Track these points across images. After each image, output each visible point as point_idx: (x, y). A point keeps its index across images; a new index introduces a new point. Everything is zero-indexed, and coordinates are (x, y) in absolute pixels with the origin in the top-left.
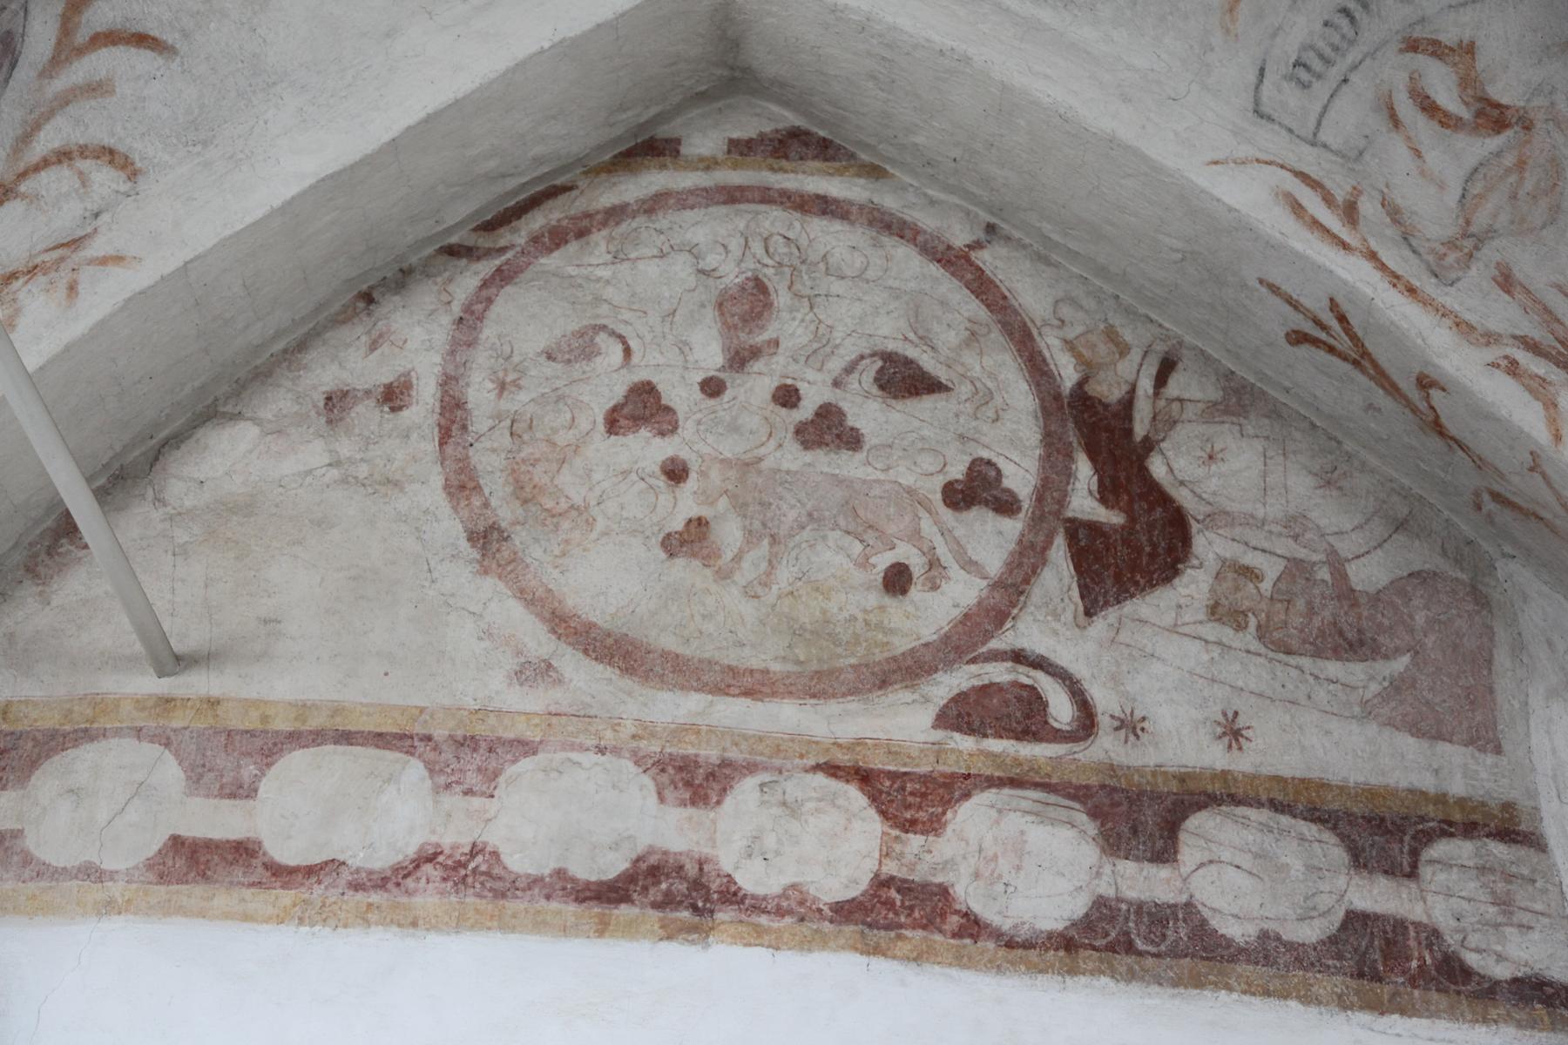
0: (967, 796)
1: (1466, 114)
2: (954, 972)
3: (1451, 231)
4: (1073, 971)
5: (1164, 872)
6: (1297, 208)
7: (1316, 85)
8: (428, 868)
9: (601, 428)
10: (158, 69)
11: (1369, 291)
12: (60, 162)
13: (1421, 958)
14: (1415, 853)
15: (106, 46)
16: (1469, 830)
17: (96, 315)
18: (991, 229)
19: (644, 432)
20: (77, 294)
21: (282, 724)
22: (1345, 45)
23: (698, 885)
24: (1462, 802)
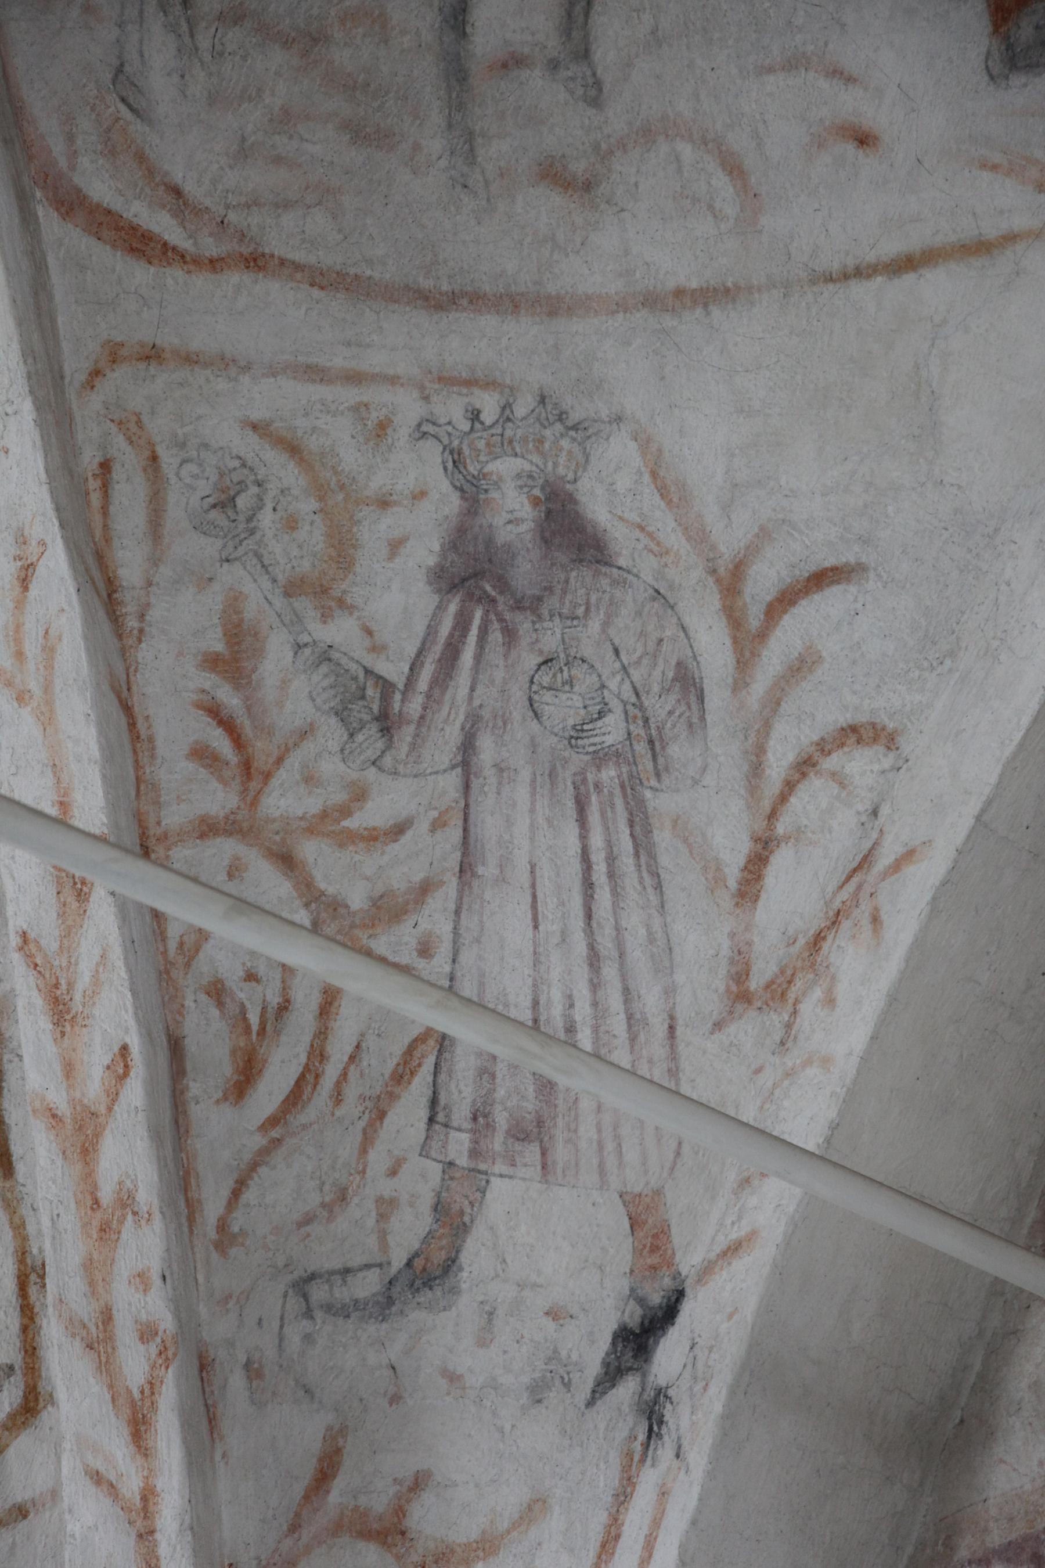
10: (855, 600)
12: (804, 775)
15: (785, 612)
17: (906, 938)
20: (881, 923)
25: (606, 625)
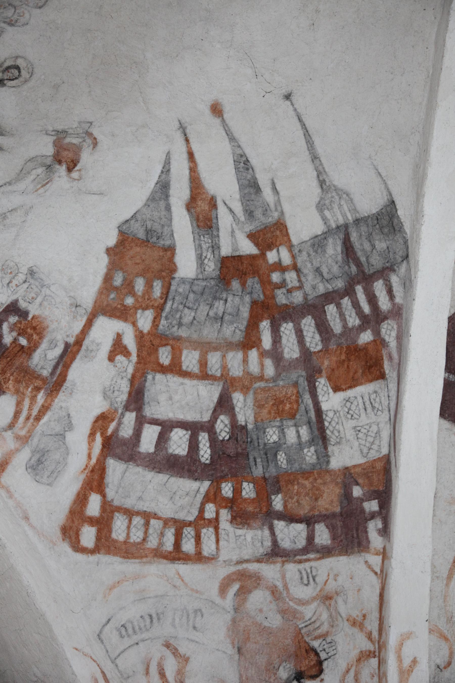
7: (126, 639)
22: (144, 629)
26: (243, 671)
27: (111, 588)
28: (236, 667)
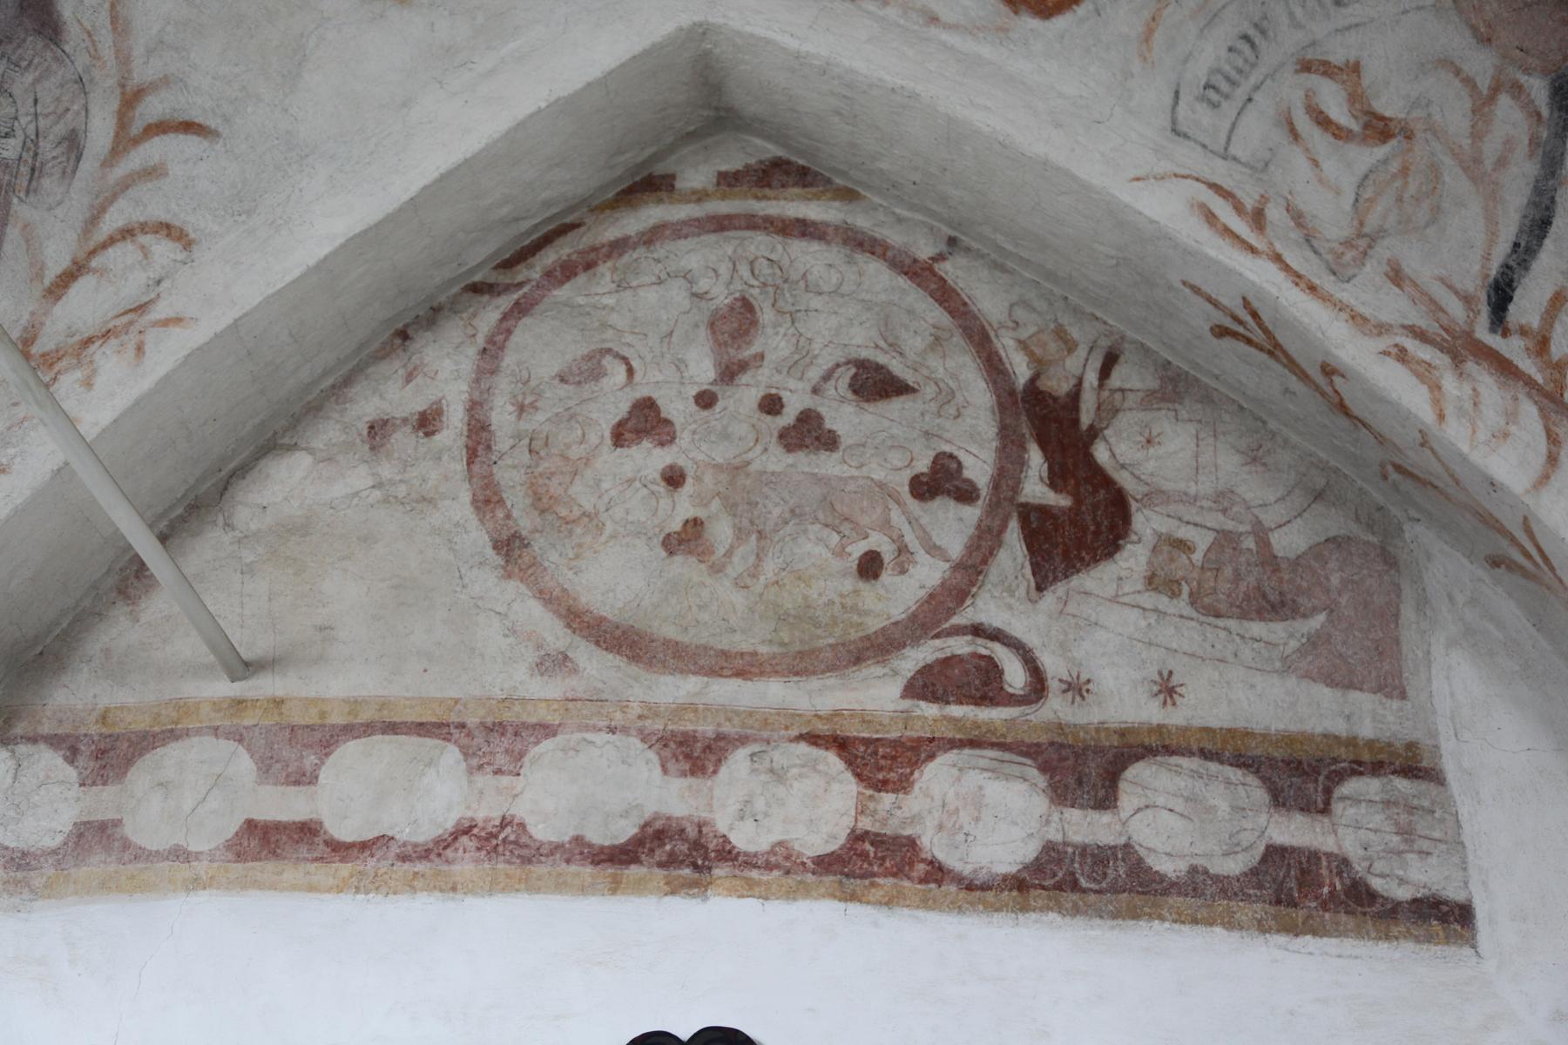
0: (931, 757)
1: (1356, 127)
2: (921, 913)
3: (1347, 232)
4: (1024, 908)
5: (1106, 818)
6: (1210, 217)
7: (1225, 104)
8: (464, 839)
9: (608, 441)
10: (204, 151)
11: (1274, 291)
12: (124, 238)
13: (1332, 885)
14: (1328, 792)
16: (1377, 768)
17: (161, 371)
18: (952, 241)
19: (646, 444)
20: (144, 353)
21: (337, 718)
22: (1247, 68)
23: (698, 845)
24: (1370, 744)
25: (37, 81)
26: (1472, 16)
27: (1147, 37)
28: (1457, 20)
